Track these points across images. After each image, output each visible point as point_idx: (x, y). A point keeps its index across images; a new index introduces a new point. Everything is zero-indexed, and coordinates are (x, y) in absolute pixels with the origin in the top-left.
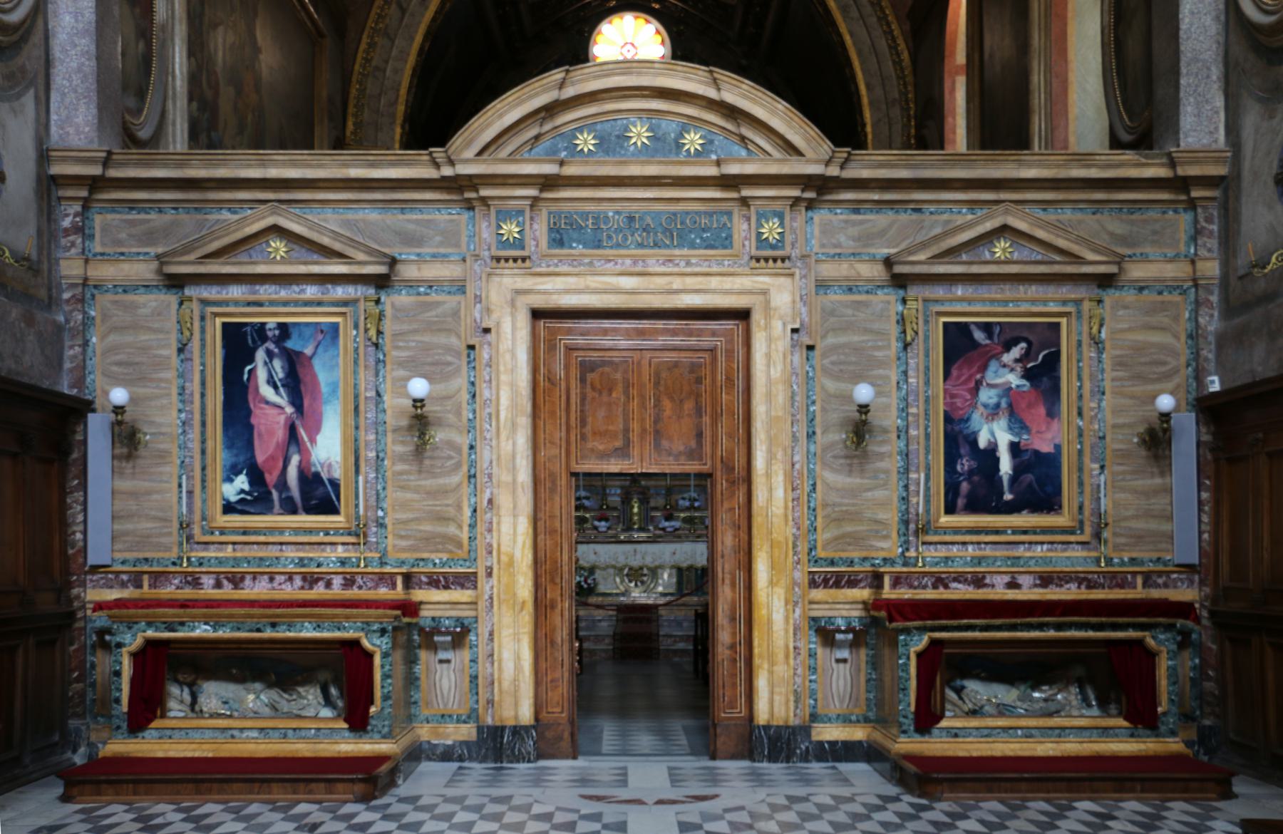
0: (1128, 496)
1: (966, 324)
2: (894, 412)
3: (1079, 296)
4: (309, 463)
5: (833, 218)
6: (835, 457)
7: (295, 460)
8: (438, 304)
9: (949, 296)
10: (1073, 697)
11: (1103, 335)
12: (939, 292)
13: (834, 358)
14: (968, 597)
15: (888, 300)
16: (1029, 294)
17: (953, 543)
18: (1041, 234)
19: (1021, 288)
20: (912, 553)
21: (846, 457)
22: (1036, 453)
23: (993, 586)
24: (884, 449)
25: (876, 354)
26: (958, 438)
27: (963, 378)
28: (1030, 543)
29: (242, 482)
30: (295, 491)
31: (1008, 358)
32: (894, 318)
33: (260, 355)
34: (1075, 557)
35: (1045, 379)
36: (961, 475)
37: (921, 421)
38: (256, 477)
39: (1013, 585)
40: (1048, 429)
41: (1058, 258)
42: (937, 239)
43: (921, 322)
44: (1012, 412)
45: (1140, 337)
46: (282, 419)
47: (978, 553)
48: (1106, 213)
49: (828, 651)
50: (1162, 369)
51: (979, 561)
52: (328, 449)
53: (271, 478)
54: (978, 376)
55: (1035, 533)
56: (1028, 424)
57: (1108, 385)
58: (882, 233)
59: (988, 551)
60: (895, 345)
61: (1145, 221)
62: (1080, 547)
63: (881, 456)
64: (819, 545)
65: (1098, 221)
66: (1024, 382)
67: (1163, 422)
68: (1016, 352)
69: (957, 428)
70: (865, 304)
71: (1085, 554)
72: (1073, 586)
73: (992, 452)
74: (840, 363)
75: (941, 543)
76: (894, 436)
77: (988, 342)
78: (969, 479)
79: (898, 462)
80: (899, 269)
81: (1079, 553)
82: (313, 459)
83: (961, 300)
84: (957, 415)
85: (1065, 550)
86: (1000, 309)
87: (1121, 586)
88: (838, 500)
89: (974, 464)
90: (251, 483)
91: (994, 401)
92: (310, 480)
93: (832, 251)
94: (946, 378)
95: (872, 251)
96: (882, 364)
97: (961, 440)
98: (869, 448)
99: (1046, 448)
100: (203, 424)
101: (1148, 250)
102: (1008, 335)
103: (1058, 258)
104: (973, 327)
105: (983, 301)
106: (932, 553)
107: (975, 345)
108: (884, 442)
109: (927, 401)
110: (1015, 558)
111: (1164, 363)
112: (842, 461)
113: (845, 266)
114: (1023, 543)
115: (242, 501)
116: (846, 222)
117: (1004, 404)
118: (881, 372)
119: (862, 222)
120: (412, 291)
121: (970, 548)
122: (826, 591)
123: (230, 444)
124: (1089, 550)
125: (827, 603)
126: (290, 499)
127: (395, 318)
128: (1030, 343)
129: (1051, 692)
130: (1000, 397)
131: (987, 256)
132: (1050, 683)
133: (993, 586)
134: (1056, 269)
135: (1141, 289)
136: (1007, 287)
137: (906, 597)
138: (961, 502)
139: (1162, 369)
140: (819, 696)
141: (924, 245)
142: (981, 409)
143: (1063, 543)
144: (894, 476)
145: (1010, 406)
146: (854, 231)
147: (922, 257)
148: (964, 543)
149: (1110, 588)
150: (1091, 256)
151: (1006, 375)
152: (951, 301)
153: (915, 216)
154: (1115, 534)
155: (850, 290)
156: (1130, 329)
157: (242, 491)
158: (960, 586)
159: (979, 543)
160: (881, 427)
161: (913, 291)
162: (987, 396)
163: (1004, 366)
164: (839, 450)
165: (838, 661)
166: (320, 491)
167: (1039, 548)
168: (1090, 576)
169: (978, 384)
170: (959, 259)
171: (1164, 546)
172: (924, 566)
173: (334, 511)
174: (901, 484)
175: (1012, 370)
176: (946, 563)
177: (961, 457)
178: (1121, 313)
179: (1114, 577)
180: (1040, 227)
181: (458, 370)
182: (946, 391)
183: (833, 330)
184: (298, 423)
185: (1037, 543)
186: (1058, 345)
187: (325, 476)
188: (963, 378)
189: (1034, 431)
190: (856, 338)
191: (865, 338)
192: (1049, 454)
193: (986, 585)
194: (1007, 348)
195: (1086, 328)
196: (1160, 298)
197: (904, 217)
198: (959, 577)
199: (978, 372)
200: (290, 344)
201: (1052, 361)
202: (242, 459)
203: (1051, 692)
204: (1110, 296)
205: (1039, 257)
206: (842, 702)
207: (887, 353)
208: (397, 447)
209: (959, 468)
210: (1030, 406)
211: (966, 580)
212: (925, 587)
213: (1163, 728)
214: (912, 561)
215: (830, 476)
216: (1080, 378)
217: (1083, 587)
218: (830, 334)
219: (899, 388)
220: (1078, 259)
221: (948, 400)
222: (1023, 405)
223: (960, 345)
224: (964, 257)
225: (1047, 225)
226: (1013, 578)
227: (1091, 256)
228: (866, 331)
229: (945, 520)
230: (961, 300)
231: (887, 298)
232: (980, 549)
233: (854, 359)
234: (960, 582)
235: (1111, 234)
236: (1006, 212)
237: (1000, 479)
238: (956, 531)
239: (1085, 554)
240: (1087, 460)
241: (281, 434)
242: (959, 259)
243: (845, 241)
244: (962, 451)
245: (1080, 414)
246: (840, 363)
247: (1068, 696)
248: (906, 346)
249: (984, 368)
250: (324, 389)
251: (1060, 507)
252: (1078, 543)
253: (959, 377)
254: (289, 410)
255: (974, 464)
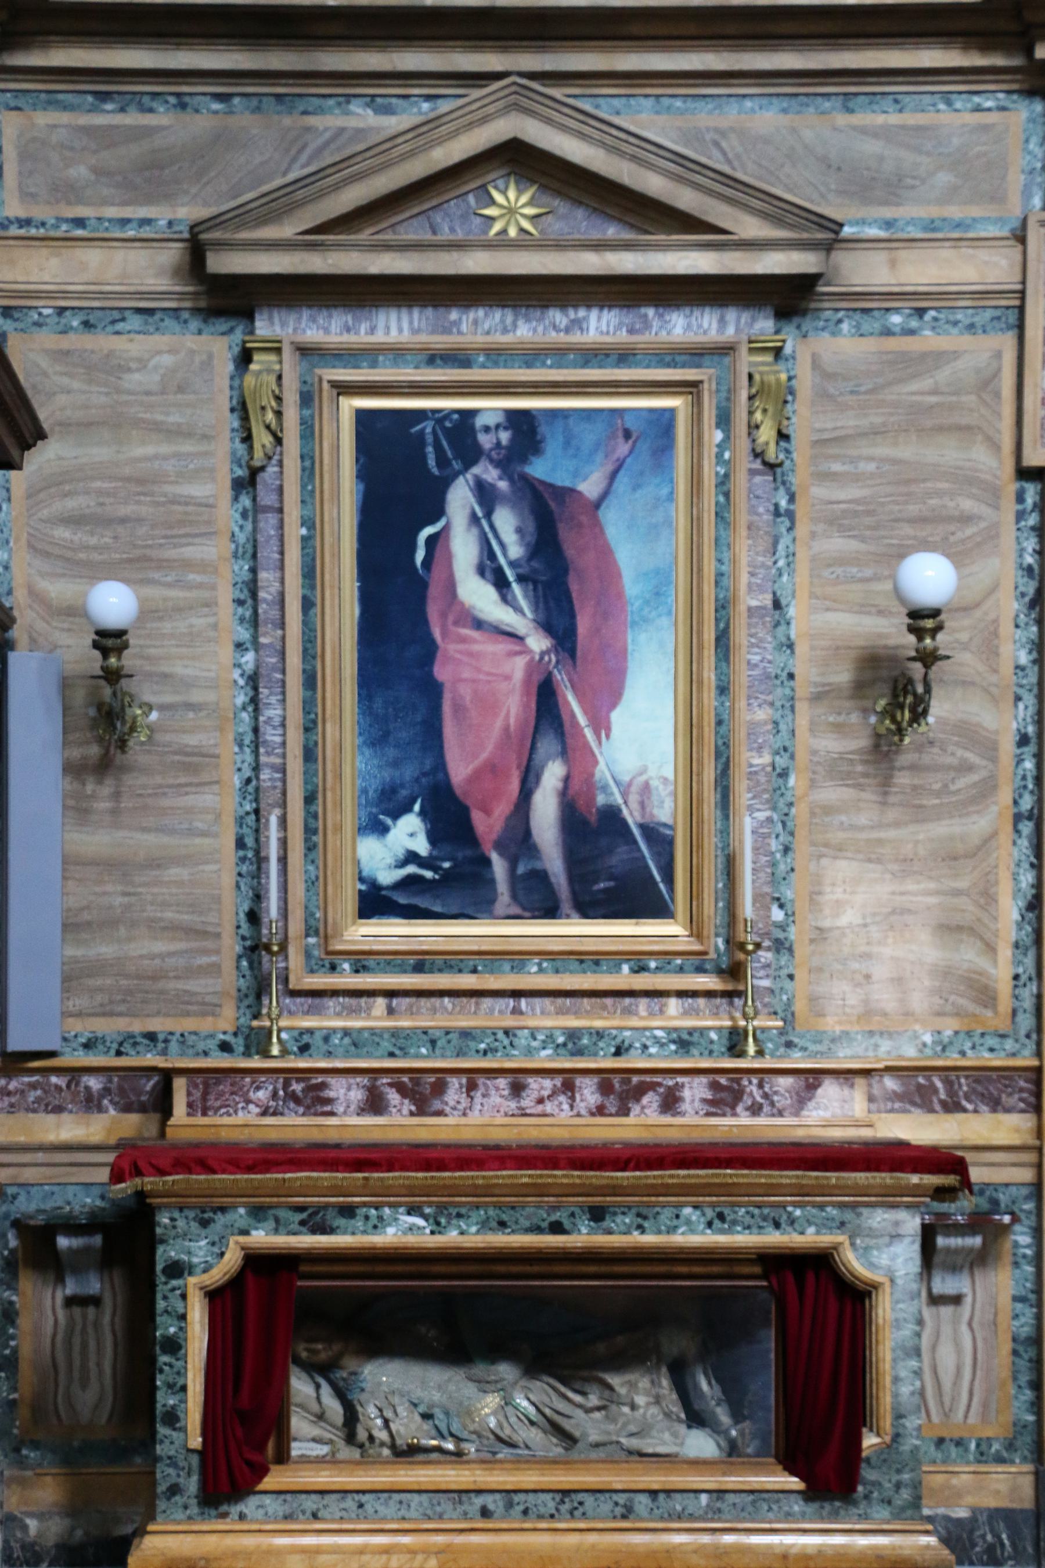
4: (590, 785)
7: (553, 774)
8: (940, 358)
29: (409, 833)
30: (552, 857)
33: (460, 498)
38: (449, 818)
46: (518, 667)
52: (640, 745)
53: (488, 824)
82: (602, 771)
90: (433, 838)
92: (592, 828)
100: (310, 681)
115: (408, 883)
120: (869, 324)
123: (377, 733)
126: (541, 877)
127: (822, 395)
157: (411, 857)
166: (619, 858)
173: (661, 910)
181: (992, 535)
184: (560, 677)
187: (632, 817)
200: (538, 469)
202: (409, 772)
208: (830, 737)
241: (514, 706)
250: (632, 587)
254: (538, 643)
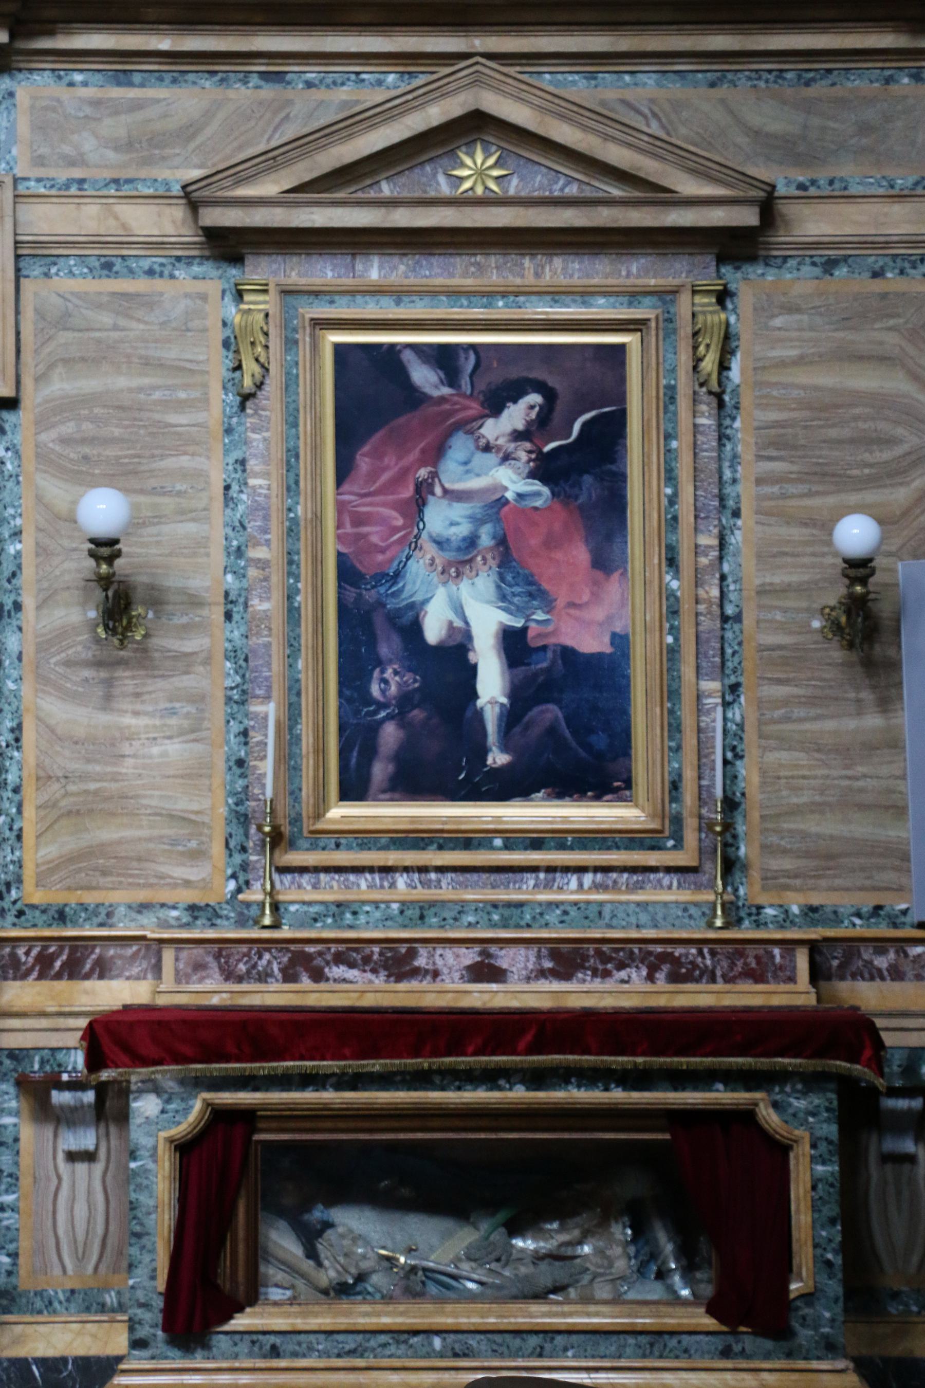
0: (801, 757)
1: (392, 347)
2: (218, 558)
3: (670, 281)
5: (59, 91)
6: (68, 663)
9: (348, 281)
10: (618, 1250)
11: (735, 374)
12: (324, 271)
13: (68, 428)
14: (369, 1001)
15: (202, 289)
16: (547, 277)
17: (358, 870)
18: (564, 133)
19: (527, 262)
20: (255, 895)
21: (98, 664)
22: (568, 654)
23: (436, 974)
24: (192, 644)
25: (173, 418)
26: (370, 619)
27: (385, 477)
28: (551, 869)
31: (495, 429)
32: (218, 335)
34: (667, 905)
35: (588, 479)
36: (381, 706)
37: (276, 578)
39: (485, 971)
40: (596, 597)
41: (616, 192)
42: (303, 145)
43: (275, 343)
44: (506, 555)
45: (826, 379)
47: (422, 894)
48: (743, 82)
49: (49, 1131)
50: (886, 455)
51: (422, 912)
54: (423, 473)
55: (562, 846)
56: (545, 586)
57: (745, 493)
58: (188, 132)
59: (446, 890)
60: (220, 401)
61: (842, 102)
62: (675, 879)
63: (185, 662)
64: (29, 874)
65: (722, 101)
66: (536, 486)
67: (854, 580)
68: (516, 415)
69: (370, 596)
70: (148, 302)
71: (685, 896)
72: (636, 975)
73: (456, 655)
74: (84, 441)
75: (327, 869)
76: (217, 615)
77: (446, 391)
78: (400, 717)
79: (226, 675)
80: (216, 217)
81: (669, 894)
83: (377, 291)
84: (368, 565)
85: (639, 886)
86: (478, 313)
87: (758, 976)
88: (77, 766)
89: (413, 681)
91: (464, 529)
93: (62, 175)
94: (340, 480)
95: (163, 173)
96: (186, 443)
97: (379, 621)
98: (156, 642)
99: (591, 642)
101: (846, 170)
102: (496, 375)
103: (616, 192)
104: (408, 356)
105: (433, 293)
106: (298, 893)
107: (414, 398)
108: (186, 629)
109: (292, 531)
110: (509, 905)
111: (890, 441)
112: (87, 673)
113: (92, 210)
114: (534, 869)
116: (97, 103)
117: (486, 540)
118: (185, 461)
119: (137, 106)
121: (401, 881)
122: (46, 985)
124: (698, 887)
125: (43, 1014)
128: (550, 395)
129: (564, 1237)
130: (477, 521)
131: (445, 189)
132: (563, 1213)
133: (436, 974)
134: (604, 217)
135: (830, 265)
136: (493, 260)
137: (215, 1000)
138: (380, 771)
139: (886, 455)
140: (24, 1244)
141: (270, 160)
142: (430, 550)
143: (633, 870)
144: (218, 711)
145: (502, 542)
146: (116, 126)
147: (269, 187)
148: (386, 870)
149: (727, 980)
150: (689, 187)
151: (490, 468)
152: (352, 293)
153: (268, 92)
154: (765, 848)
155: (108, 266)
156: (800, 361)
158: (353, 974)
159: (423, 869)
160: (183, 591)
161: (263, 269)
162: (443, 519)
163: (487, 448)
164: (80, 647)
165: (72, 1157)
167: (574, 880)
168: (678, 951)
169: (422, 493)
170: (372, 194)
171: (888, 877)
172: (276, 926)
174: (235, 727)
175: (506, 458)
176: (337, 917)
177: (380, 663)
178: (778, 322)
179: (741, 954)
180: (562, 117)
182: (341, 507)
183: (66, 361)
185: (567, 869)
186: (621, 398)
188: (385, 477)
189: (561, 603)
190: (122, 382)
191: (146, 381)
192: (599, 656)
193: (416, 973)
194: (495, 405)
195: (684, 359)
196: (877, 286)
197: (244, 95)
198: (350, 953)
199: (423, 463)
201: (607, 436)
203: (564, 1237)
204: (750, 284)
205: (573, 190)
206: (80, 1259)
207: (200, 417)
209: (375, 690)
210: (551, 543)
211: (367, 960)
212: (264, 977)
213: (804, 1335)
214: (254, 911)
215: (56, 709)
216: (670, 477)
217: (661, 976)
218: (60, 369)
219: (228, 500)
220: (658, 194)
221: (348, 529)
222: (534, 542)
223: (378, 401)
224: (386, 190)
225: (575, 112)
226: (485, 953)
227: (689, 187)
228: (148, 364)
229: (340, 813)
230: (377, 291)
231: (200, 286)
232: (426, 884)
233: (117, 432)
234: (352, 965)
235: (756, 134)
236: (477, 82)
237: (479, 715)
238: (366, 838)
239: (685, 896)
240: (688, 671)
242: (372, 194)
243: (96, 151)
244: (384, 650)
245: (672, 562)
246: (84, 441)
247: (604, 1249)
248: (245, 398)
249: (436, 453)
251: (628, 784)
252: (669, 870)
253: (373, 475)
255: (413, 681)
